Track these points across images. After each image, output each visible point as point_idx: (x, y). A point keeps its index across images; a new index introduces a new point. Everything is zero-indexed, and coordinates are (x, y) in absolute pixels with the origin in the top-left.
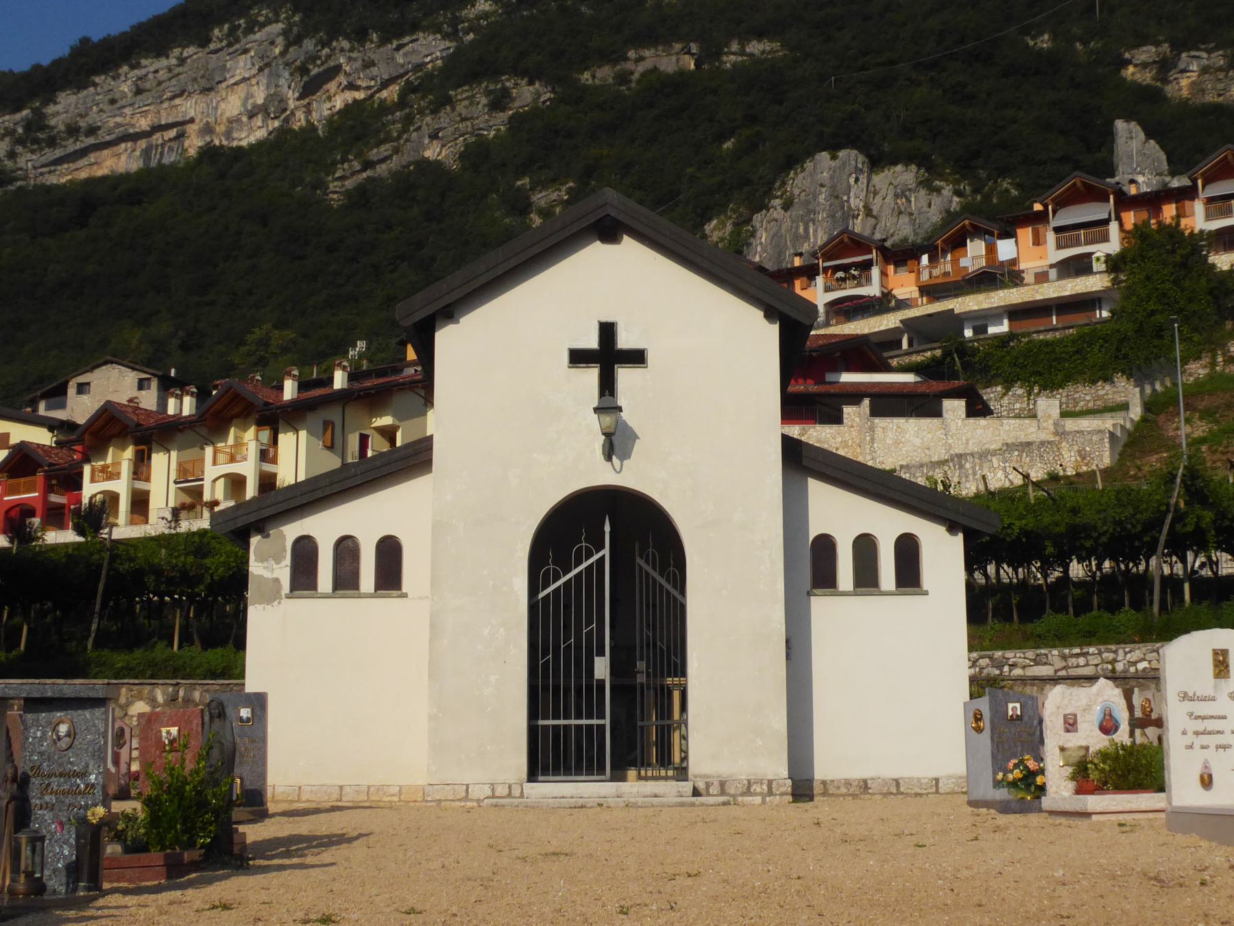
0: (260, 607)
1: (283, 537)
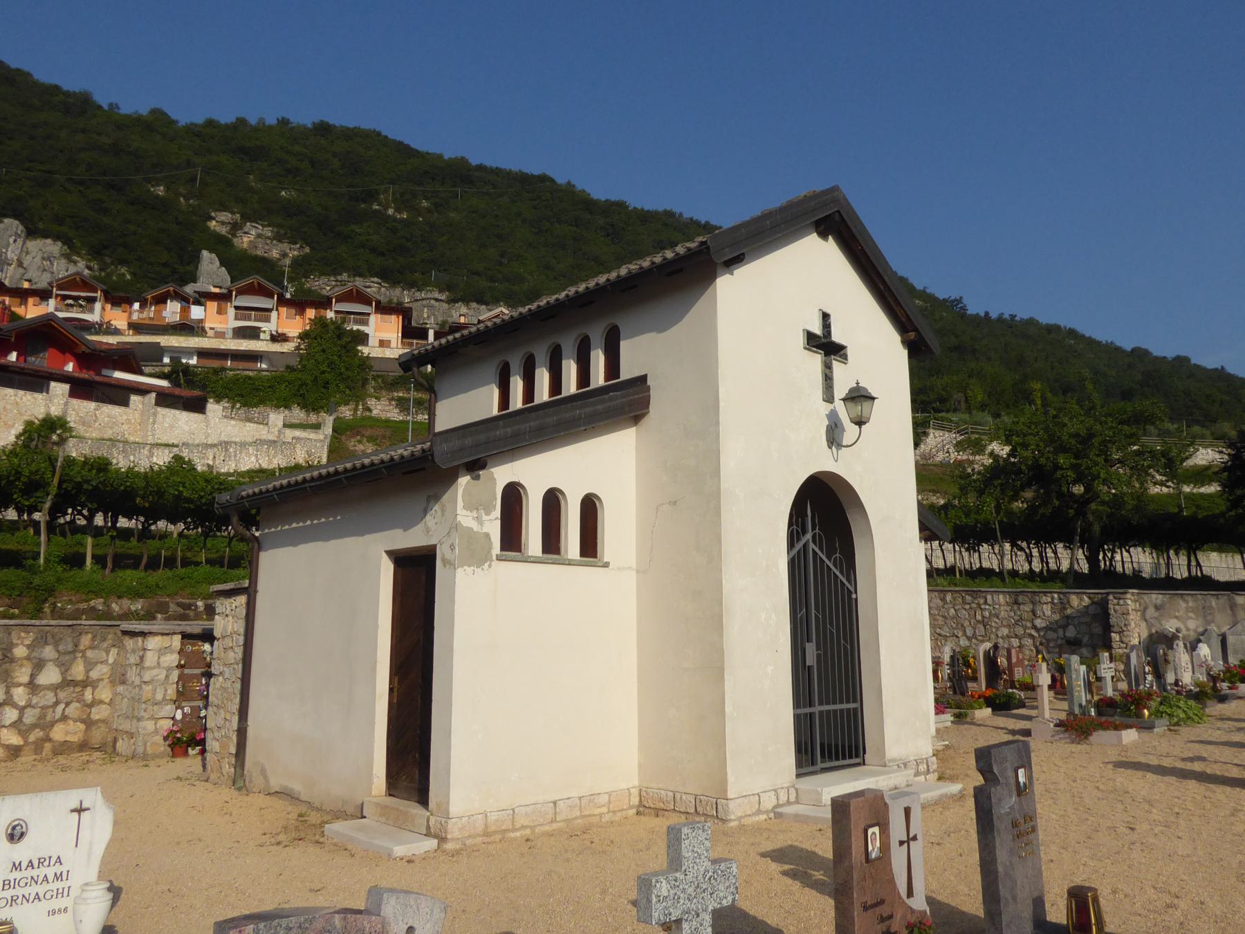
0: (469, 570)
1: (493, 480)
